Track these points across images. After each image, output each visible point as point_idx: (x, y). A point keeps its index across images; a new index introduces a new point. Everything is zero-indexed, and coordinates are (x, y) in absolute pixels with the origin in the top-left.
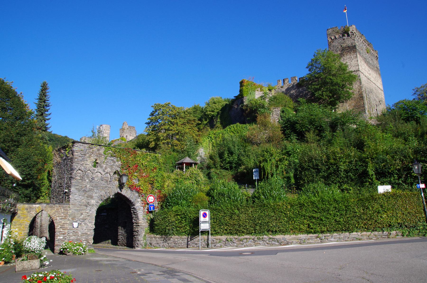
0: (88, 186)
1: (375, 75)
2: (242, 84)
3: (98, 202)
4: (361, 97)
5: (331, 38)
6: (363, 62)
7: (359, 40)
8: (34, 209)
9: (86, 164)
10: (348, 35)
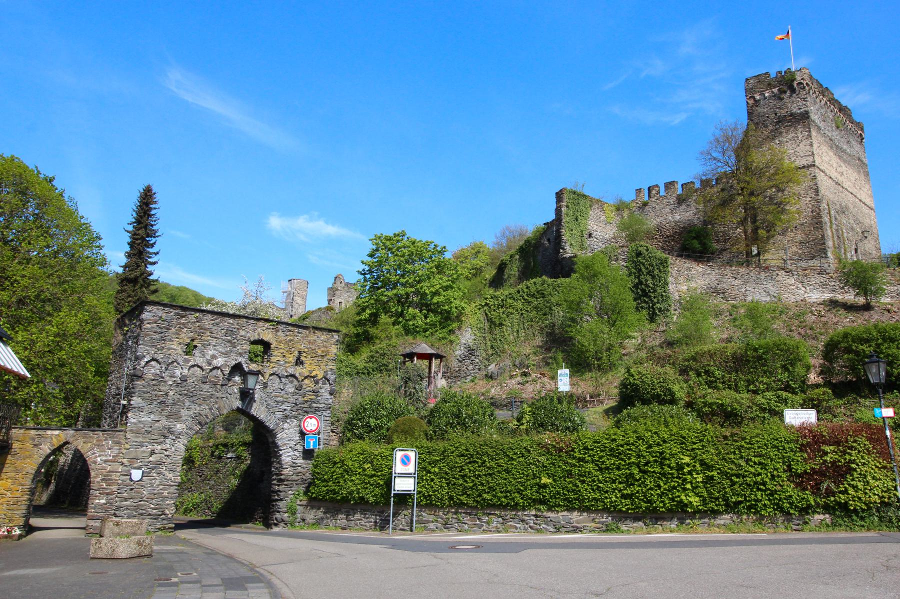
0: (171, 393)
1: (855, 174)
2: (559, 196)
3: (191, 429)
4: (817, 221)
5: (753, 97)
6: (825, 148)
7: (818, 100)
8: (49, 440)
9: (169, 349)
10: (793, 91)
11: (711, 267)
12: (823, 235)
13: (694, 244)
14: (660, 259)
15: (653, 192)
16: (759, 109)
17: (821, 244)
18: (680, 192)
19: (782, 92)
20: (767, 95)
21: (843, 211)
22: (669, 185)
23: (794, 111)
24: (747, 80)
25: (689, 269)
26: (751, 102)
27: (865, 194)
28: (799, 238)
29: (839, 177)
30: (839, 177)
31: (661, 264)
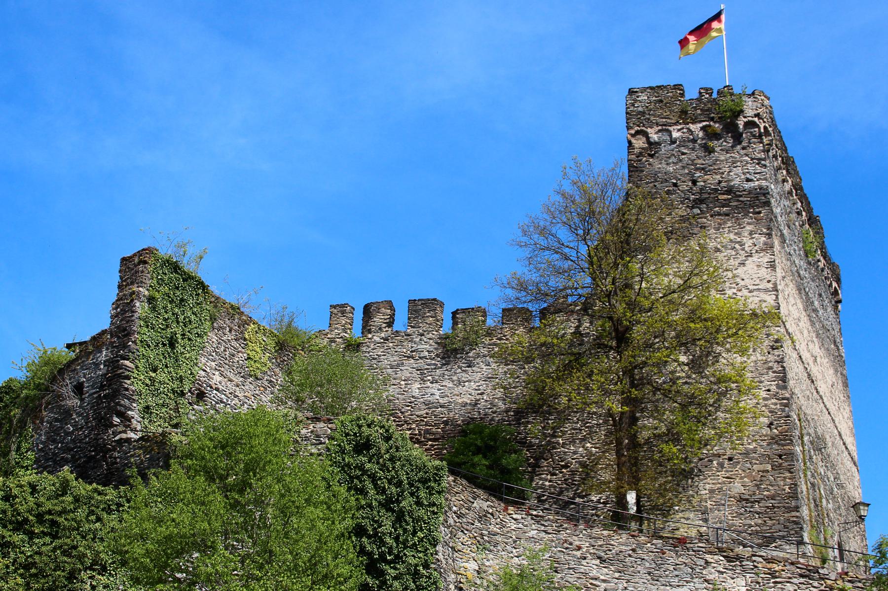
5: (646, 134)
11: (537, 519)
12: (794, 486)
13: (492, 458)
14: (422, 468)
15: (378, 320)
16: (657, 165)
17: (789, 510)
18: (446, 328)
20: (675, 135)
22: (421, 308)
23: (736, 182)
24: (631, 92)
25: (483, 517)
26: (639, 143)
28: (737, 488)
29: (811, 363)
30: (811, 363)
31: (424, 481)
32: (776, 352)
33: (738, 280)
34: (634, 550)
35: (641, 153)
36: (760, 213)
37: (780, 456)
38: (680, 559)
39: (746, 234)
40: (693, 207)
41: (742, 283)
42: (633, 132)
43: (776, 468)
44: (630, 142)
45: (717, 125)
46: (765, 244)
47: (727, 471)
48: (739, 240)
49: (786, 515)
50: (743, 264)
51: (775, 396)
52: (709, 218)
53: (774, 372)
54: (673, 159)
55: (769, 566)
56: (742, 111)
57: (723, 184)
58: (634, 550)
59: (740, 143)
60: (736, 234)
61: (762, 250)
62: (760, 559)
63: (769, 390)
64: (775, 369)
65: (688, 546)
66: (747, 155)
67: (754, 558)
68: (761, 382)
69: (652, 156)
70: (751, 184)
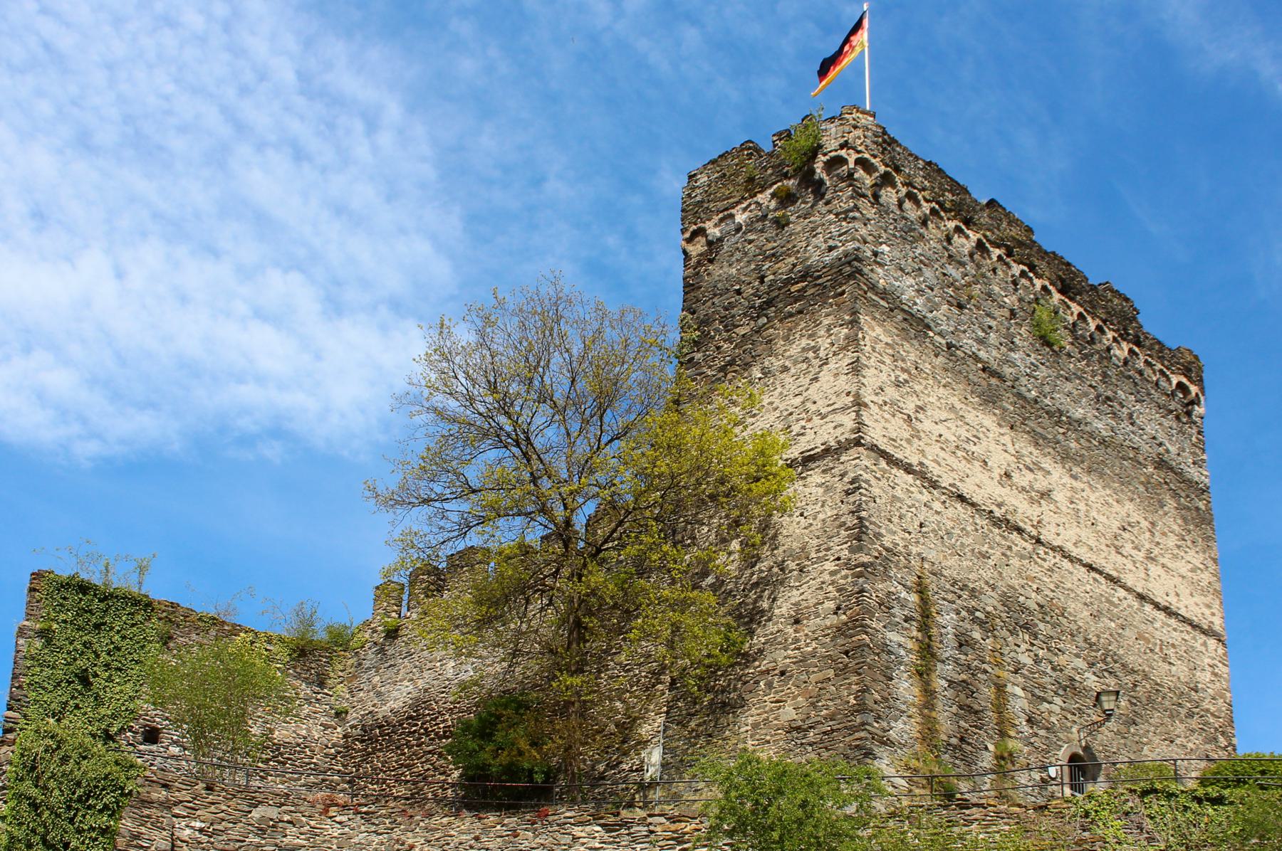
10: (818, 189)
19: (786, 199)
21: (1019, 618)
23: (814, 258)
24: (691, 177)
27: (1179, 575)
28: (788, 713)
32: (851, 499)
33: (809, 405)
34: (477, 839)
35: (699, 262)
36: (843, 293)
37: (846, 653)
38: (537, 840)
39: (822, 333)
40: (758, 317)
41: (813, 408)
42: (687, 235)
43: (842, 671)
44: (685, 252)
45: (792, 182)
46: (847, 337)
47: (776, 692)
48: (813, 344)
49: (847, 739)
50: (816, 379)
51: (847, 565)
52: (778, 325)
53: (846, 530)
54: (738, 255)
55: (673, 827)
56: (820, 146)
57: (799, 268)
58: (477, 839)
59: (822, 196)
60: (810, 336)
61: (841, 349)
62: (662, 820)
63: (838, 559)
64: (849, 524)
65: (550, 818)
66: (830, 212)
67: (650, 820)
68: (828, 549)
69: (711, 261)
70: (834, 254)
